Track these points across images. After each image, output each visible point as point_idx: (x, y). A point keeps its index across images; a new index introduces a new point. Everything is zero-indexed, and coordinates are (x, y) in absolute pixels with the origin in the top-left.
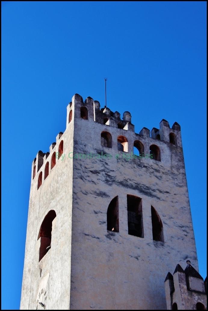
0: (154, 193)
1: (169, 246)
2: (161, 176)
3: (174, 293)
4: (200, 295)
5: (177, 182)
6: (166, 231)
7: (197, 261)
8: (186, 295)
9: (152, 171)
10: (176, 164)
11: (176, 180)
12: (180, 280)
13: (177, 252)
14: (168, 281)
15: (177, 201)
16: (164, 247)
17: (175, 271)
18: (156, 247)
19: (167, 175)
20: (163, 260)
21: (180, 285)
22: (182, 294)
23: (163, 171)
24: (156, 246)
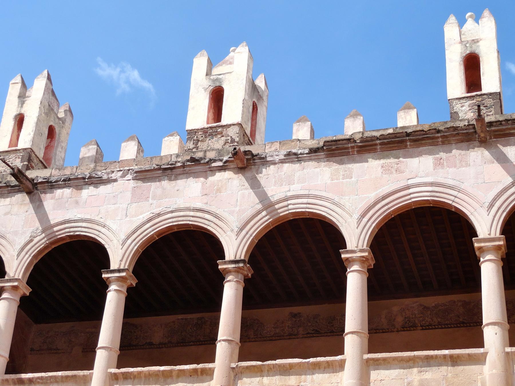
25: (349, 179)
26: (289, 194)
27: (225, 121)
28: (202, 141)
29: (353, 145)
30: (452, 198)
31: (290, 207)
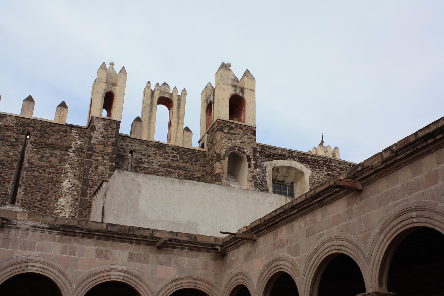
25: (74, 256)
26: (30, 258)
29: (80, 231)
30: (136, 284)
31: (29, 268)
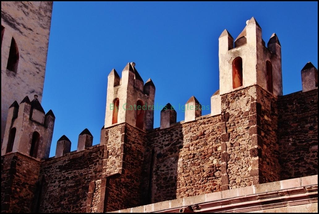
0: (18, 27)
1: (20, 78)
2: (28, 12)
3: (16, 120)
4: (39, 126)
5: (41, 22)
6: (21, 65)
7: (41, 96)
8: (27, 124)
9: (21, 5)
10: (45, 6)
11: (41, 20)
12: (26, 110)
13: (26, 85)
14: (13, 108)
15: (38, 40)
16: (15, 77)
17: (23, 102)
18: (8, 76)
19: (34, 13)
20: (11, 89)
21: (24, 114)
22: (24, 122)
23: (31, 9)
24: (8, 75)
27: (245, 85)
28: (232, 102)
